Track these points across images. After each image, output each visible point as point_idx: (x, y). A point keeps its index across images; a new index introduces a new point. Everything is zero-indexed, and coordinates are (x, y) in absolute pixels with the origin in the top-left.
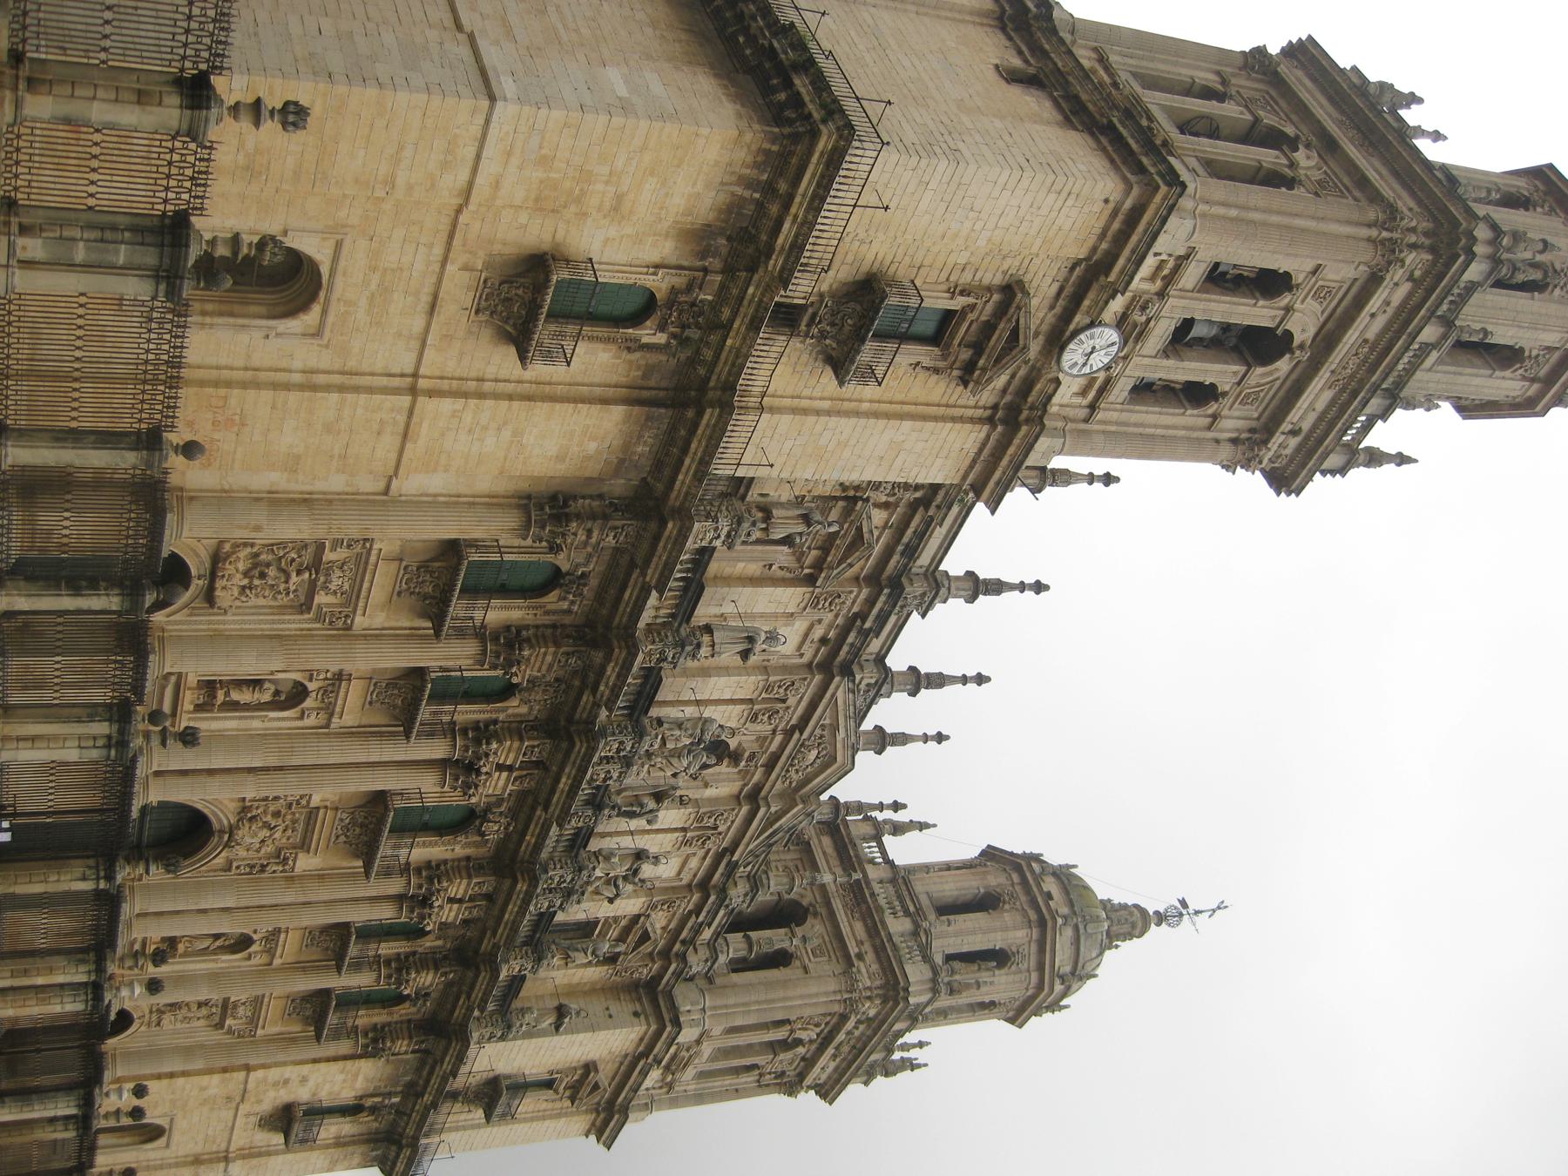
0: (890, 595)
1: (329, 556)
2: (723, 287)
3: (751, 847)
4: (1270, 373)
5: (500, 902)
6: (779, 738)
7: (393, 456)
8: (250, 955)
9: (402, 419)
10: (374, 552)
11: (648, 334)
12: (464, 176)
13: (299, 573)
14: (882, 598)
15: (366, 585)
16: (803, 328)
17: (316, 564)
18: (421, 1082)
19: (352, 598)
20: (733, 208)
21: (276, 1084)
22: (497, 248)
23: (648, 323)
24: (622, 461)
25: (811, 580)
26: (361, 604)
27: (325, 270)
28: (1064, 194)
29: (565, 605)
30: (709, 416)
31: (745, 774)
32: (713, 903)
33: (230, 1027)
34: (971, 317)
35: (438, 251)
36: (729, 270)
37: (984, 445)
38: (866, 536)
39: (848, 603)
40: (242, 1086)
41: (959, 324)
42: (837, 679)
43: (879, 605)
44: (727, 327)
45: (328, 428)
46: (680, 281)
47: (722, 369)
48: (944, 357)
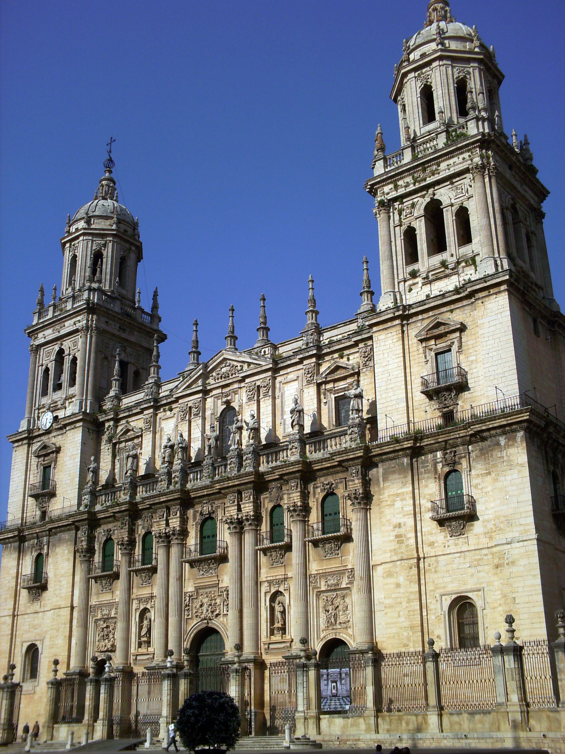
1: (99, 616)
3: (263, 363)
5: (236, 488)
6: (214, 392)
8: (284, 590)
9: (56, 610)
14: (142, 407)
15: (106, 602)
16: (45, 509)
18: (401, 453)
21: (400, 542)
22: (27, 602)
26: (112, 601)
31: (235, 392)
32: (302, 354)
33: (347, 584)
34: (43, 463)
35: (26, 616)
40: (399, 563)
42: (174, 396)
45: (58, 631)
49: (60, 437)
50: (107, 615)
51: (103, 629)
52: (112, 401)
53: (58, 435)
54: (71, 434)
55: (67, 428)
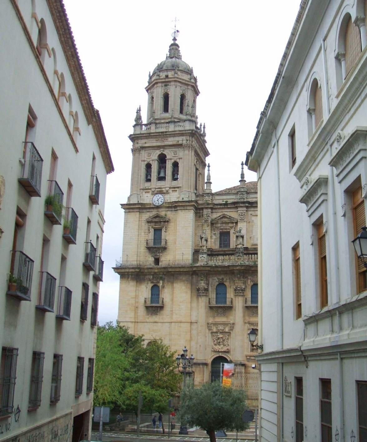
0: (237, 204)
1: (215, 330)
2: (149, 275)
4: (168, 153)
7: (186, 324)
9: (177, 324)
10: (212, 322)
11: (161, 284)
12: (129, 323)
13: (218, 336)
14: (238, 205)
15: (221, 322)
17: (217, 332)
19: (225, 324)
20: (133, 279)
23: (158, 285)
24: (187, 281)
25: (237, 223)
26: (227, 322)
27: (150, 341)
28: (127, 223)
29: (228, 280)
30: (170, 270)
36: (146, 275)
37: (182, 210)
38: (221, 217)
39: (241, 211)
41: (156, 228)
43: (241, 205)
44: (155, 273)
46: (149, 282)
47: (162, 270)
48: (164, 227)
49: (168, 212)
50: (222, 330)
51: (219, 338)
52: (209, 196)
53: (168, 211)
54: (182, 213)
55: (178, 208)
